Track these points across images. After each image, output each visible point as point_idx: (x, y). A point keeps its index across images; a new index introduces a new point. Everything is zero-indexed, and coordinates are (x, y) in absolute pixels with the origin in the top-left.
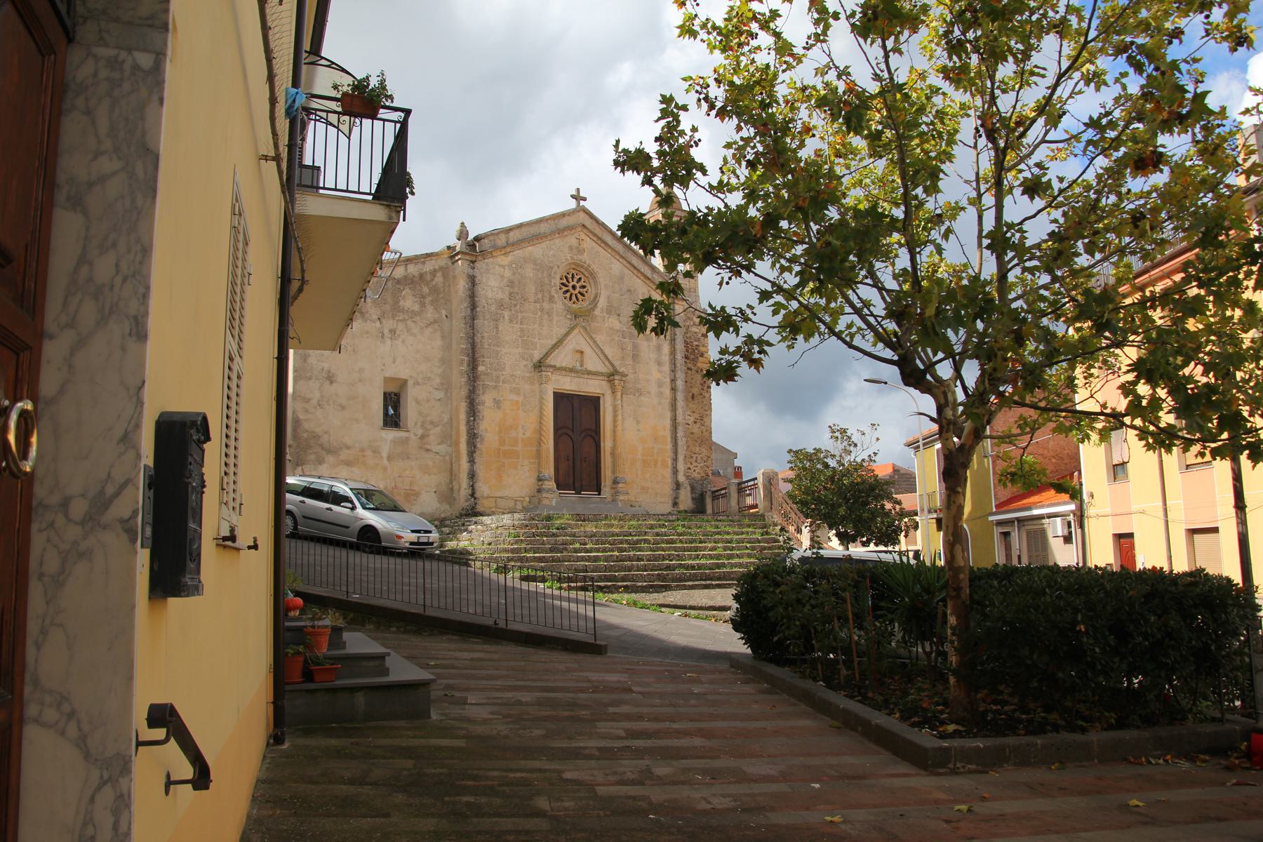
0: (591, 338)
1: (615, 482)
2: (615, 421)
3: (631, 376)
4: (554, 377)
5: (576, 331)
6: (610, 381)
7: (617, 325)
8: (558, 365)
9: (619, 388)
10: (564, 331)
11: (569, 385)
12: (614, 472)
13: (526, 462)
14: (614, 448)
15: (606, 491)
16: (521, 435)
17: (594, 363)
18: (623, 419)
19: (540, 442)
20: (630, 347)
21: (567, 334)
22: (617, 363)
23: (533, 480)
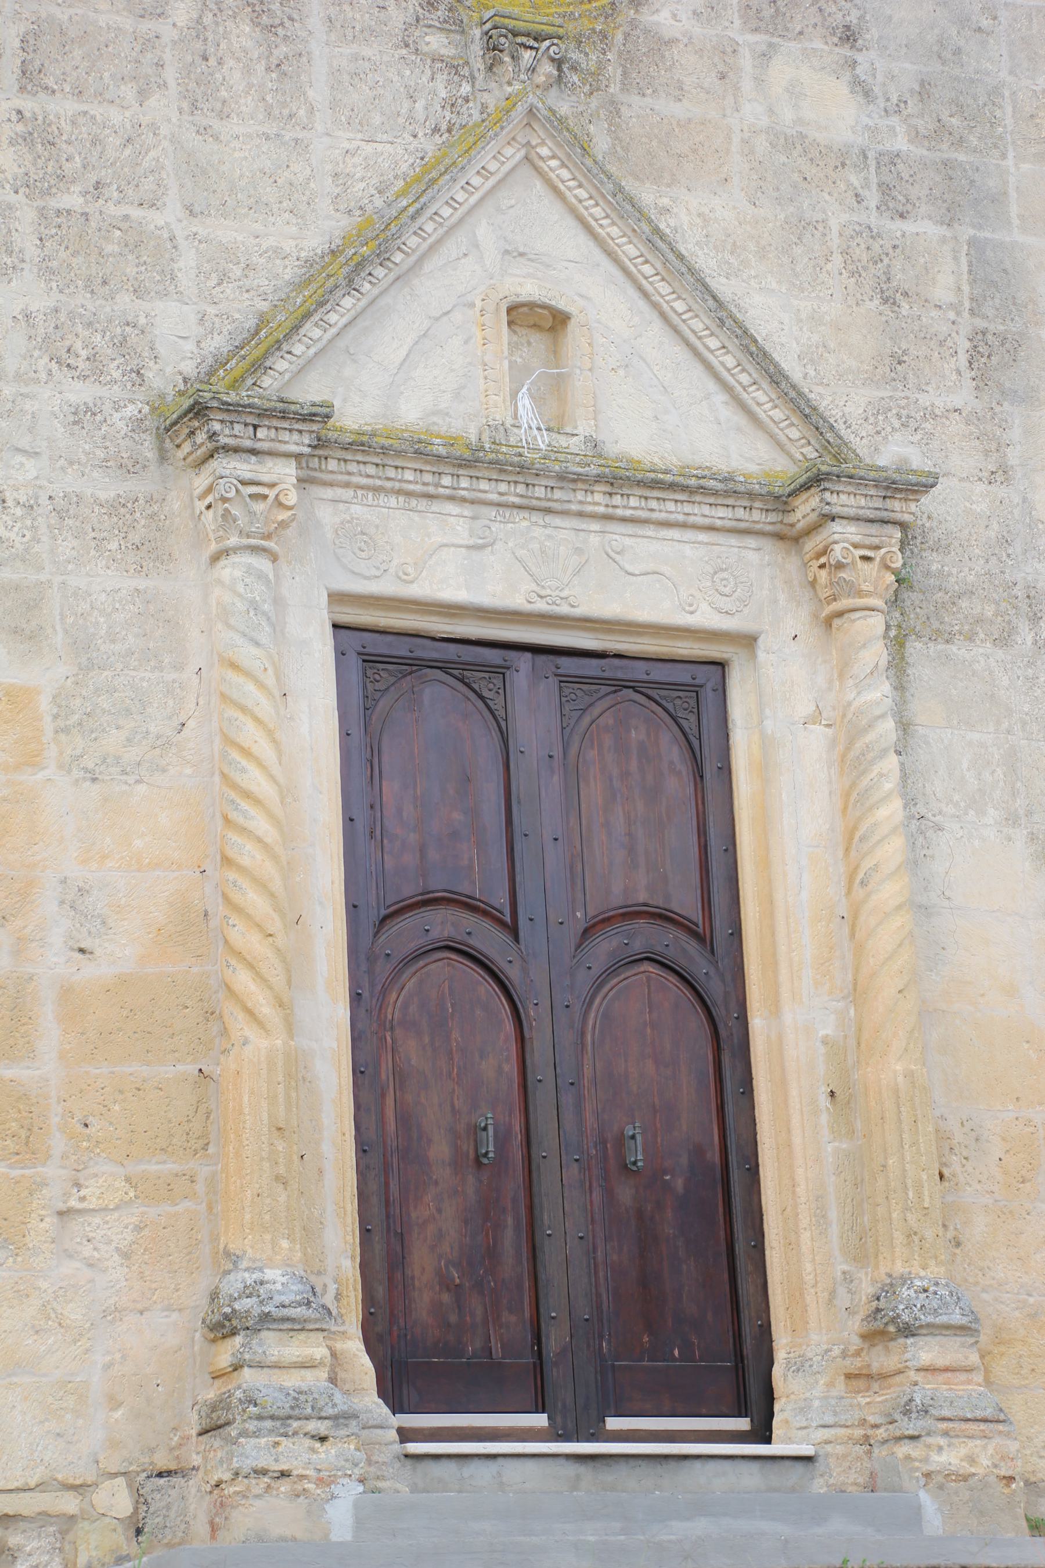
0: (626, 206)
1: (886, 1327)
2: (852, 839)
3: (955, 505)
4: (330, 511)
5: (500, 156)
6: (790, 538)
7: (835, 113)
8: (354, 414)
9: (873, 580)
10: (397, 155)
11: (465, 566)
12: (862, 1249)
13: (105, 1182)
14: (849, 1052)
15: (807, 1401)
16: (53, 962)
17: (653, 402)
18: (919, 824)
19: (210, 1016)
20: (947, 283)
21: (428, 180)
22: (847, 405)
23: (165, 1330)
